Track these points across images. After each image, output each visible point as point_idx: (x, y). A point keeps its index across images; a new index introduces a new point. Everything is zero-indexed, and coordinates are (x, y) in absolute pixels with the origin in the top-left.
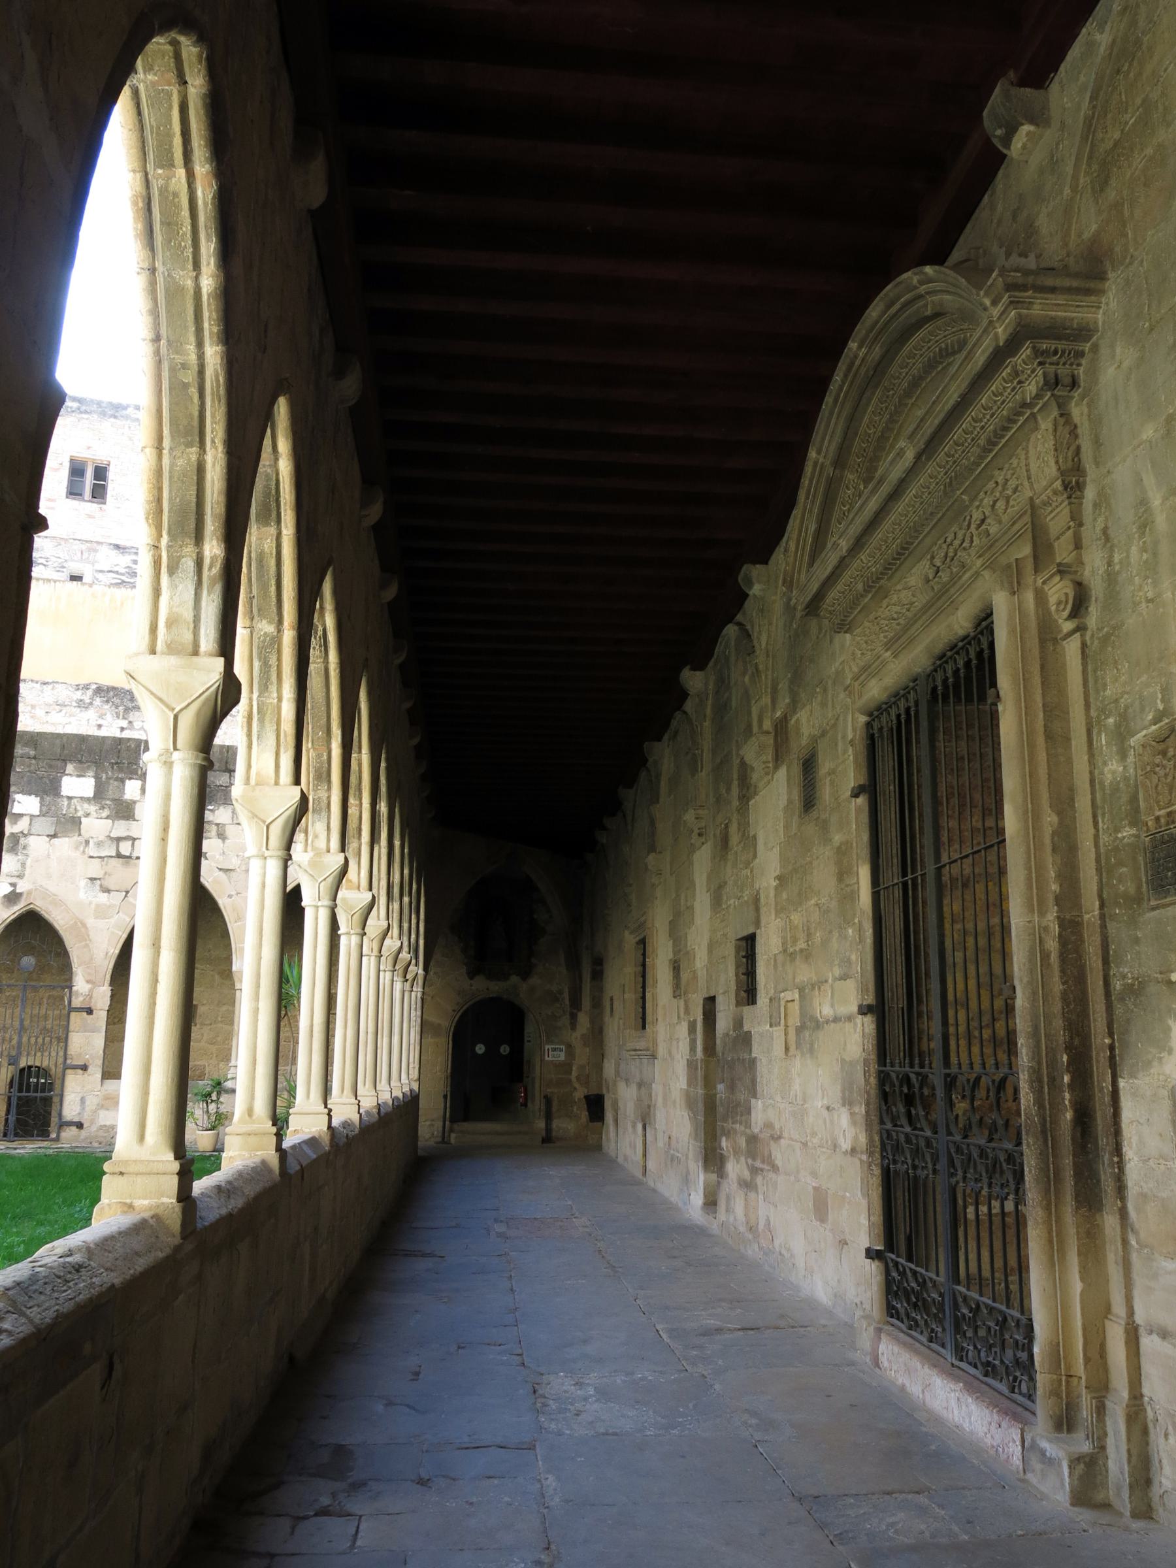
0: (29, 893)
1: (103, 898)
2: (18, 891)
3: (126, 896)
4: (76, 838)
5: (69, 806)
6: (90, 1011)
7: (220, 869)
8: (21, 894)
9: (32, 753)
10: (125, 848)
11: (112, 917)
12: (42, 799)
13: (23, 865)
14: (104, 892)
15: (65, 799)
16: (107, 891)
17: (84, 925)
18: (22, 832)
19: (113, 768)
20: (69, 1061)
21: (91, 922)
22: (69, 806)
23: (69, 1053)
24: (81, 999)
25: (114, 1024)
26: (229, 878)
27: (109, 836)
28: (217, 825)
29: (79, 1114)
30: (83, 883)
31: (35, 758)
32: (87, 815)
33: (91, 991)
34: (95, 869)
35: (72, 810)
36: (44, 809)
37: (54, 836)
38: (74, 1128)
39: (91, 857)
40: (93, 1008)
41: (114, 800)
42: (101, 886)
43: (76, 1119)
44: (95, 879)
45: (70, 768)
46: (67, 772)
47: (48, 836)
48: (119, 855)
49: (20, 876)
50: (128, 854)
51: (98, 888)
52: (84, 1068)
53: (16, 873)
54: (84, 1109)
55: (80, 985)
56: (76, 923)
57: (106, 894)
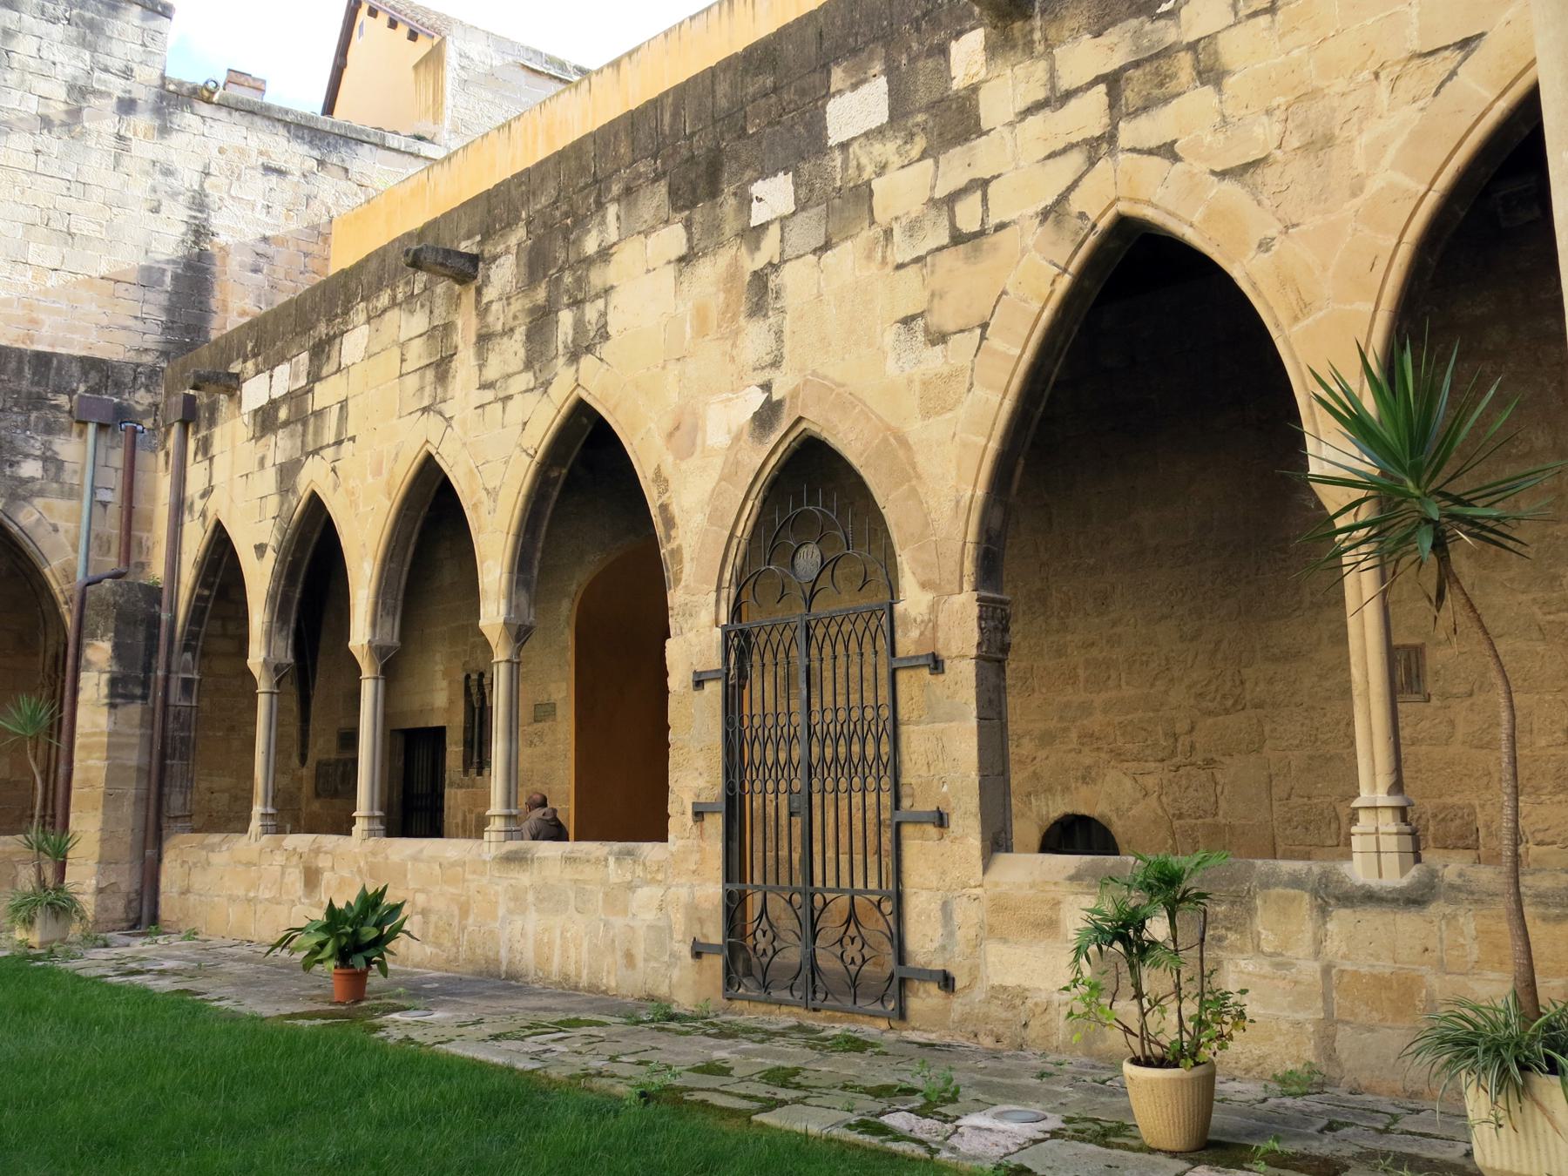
0: (794, 394)
1: (934, 359)
2: (775, 397)
3: (983, 337)
4: (867, 234)
5: (845, 162)
6: (936, 664)
7: (1223, 175)
8: (780, 403)
9: (769, 82)
10: (968, 216)
11: (958, 401)
12: (797, 175)
13: (779, 334)
14: (933, 343)
15: (837, 153)
16: (938, 338)
17: (903, 442)
18: (770, 264)
19: (918, 30)
20: (906, 803)
21: (915, 429)
22: (845, 162)
23: (904, 780)
24: (915, 633)
25: (1227, 712)
26: (1255, 192)
27: (931, 200)
28: (1192, 47)
29: (943, 948)
30: (890, 335)
31: (775, 90)
32: (882, 169)
33: (934, 608)
34: (909, 293)
35: (852, 171)
36: (803, 192)
37: (827, 246)
38: (933, 988)
39: (900, 267)
40: (943, 654)
41: (931, 107)
42: (927, 330)
43: (937, 965)
44: (913, 318)
45: (838, 76)
46: (833, 89)
47: (814, 252)
48: (958, 238)
49: (776, 364)
50: (976, 227)
51: (921, 337)
52: (941, 820)
53: (768, 359)
54: (951, 934)
55: (913, 600)
56: (885, 440)
57: (939, 348)
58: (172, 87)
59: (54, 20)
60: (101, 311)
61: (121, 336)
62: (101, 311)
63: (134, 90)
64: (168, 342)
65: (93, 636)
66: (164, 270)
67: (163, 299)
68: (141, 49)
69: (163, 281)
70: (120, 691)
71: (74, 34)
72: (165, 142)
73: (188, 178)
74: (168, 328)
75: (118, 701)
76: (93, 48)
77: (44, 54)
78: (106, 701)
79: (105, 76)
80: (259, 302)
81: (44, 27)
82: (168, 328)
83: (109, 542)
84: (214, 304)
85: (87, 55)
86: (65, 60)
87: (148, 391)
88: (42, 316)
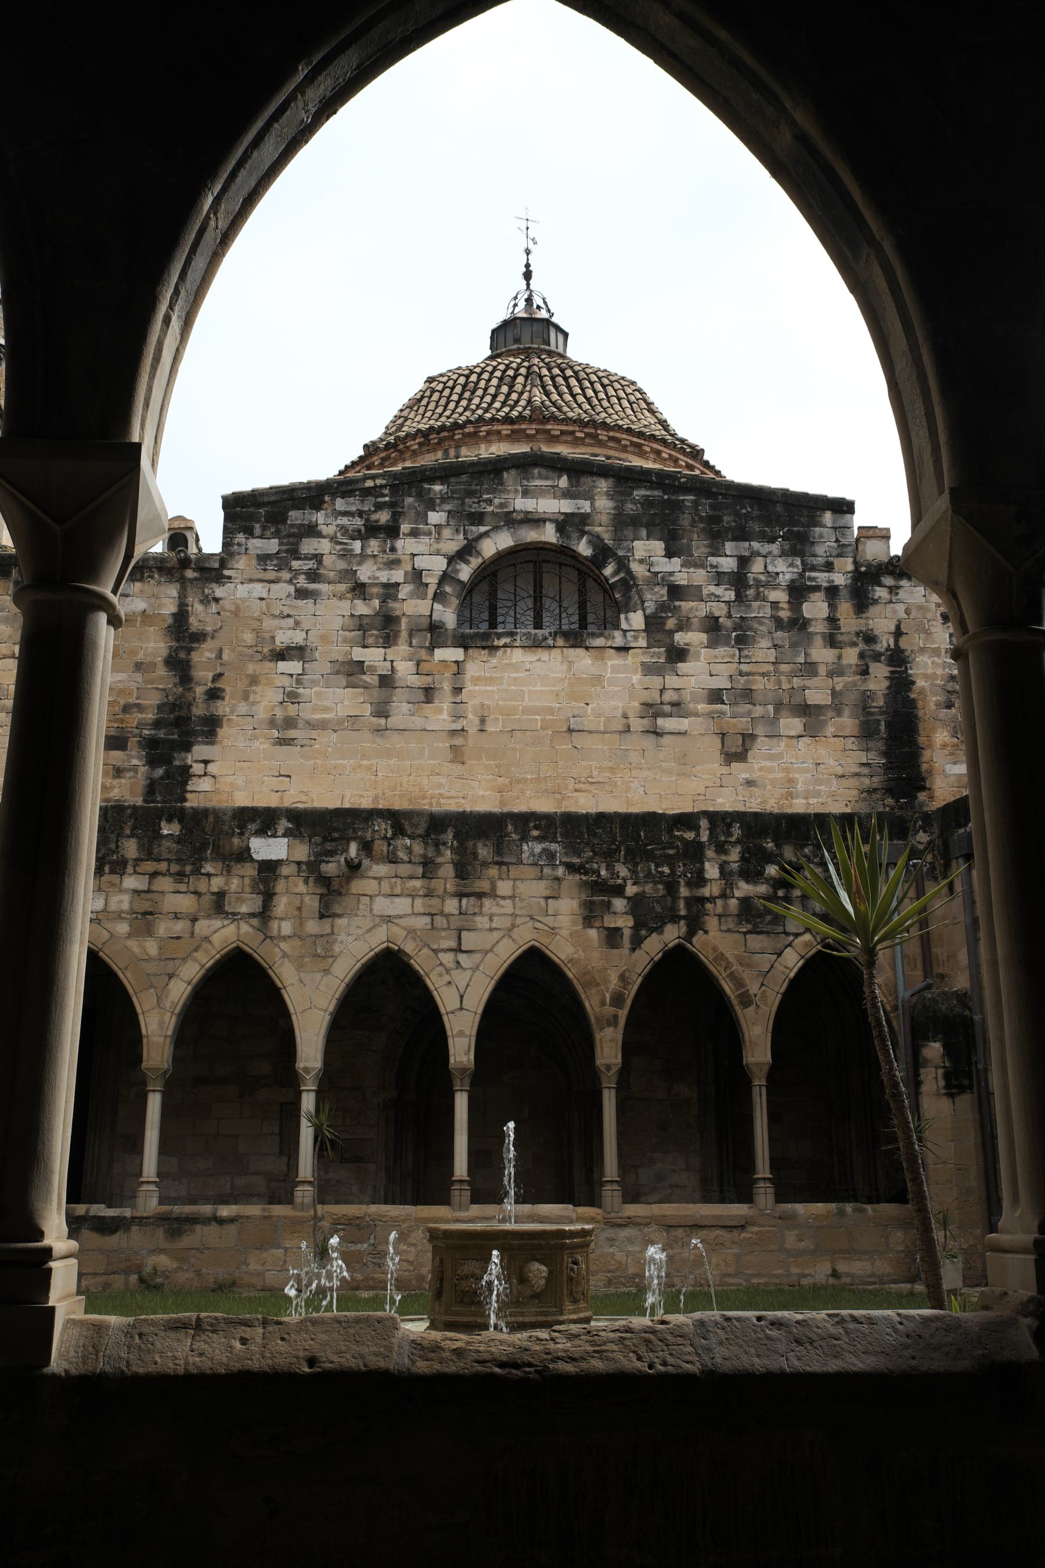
58: (863, 569)
59: (772, 540)
60: (837, 763)
61: (853, 782)
62: (837, 763)
63: (836, 579)
64: (889, 780)
65: (927, 1039)
66: (879, 721)
67: (881, 745)
68: (835, 545)
69: (880, 730)
70: (954, 1082)
71: (787, 547)
72: (863, 616)
73: (886, 641)
74: (888, 768)
75: (954, 1091)
76: (801, 554)
77: (770, 568)
78: (944, 1091)
79: (813, 574)
80: (956, 732)
81: (766, 548)
82: (887, 768)
83: (915, 959)
84: (922, 740)
85: (798, 562)
86: (784, 569)
87: (925, 832)
88: (797, 776)
